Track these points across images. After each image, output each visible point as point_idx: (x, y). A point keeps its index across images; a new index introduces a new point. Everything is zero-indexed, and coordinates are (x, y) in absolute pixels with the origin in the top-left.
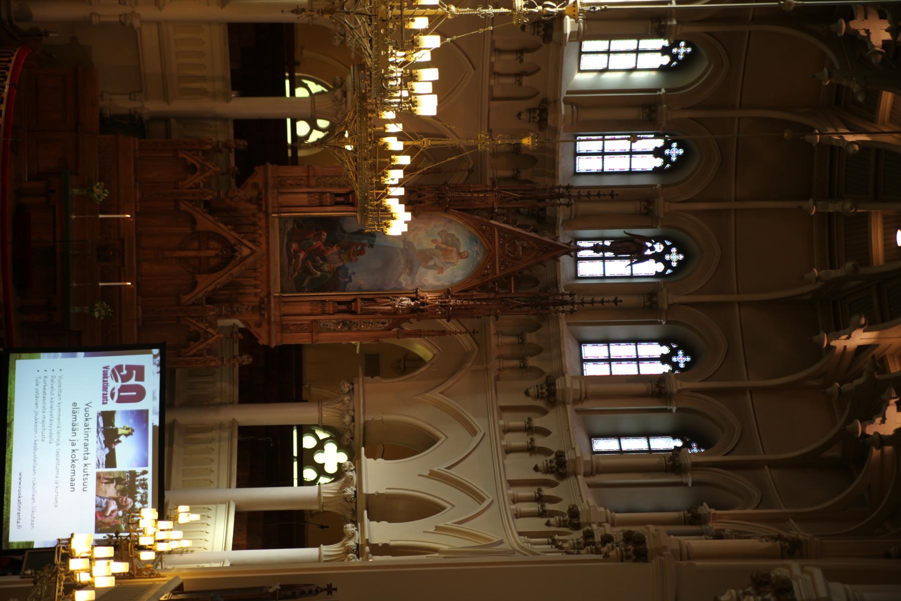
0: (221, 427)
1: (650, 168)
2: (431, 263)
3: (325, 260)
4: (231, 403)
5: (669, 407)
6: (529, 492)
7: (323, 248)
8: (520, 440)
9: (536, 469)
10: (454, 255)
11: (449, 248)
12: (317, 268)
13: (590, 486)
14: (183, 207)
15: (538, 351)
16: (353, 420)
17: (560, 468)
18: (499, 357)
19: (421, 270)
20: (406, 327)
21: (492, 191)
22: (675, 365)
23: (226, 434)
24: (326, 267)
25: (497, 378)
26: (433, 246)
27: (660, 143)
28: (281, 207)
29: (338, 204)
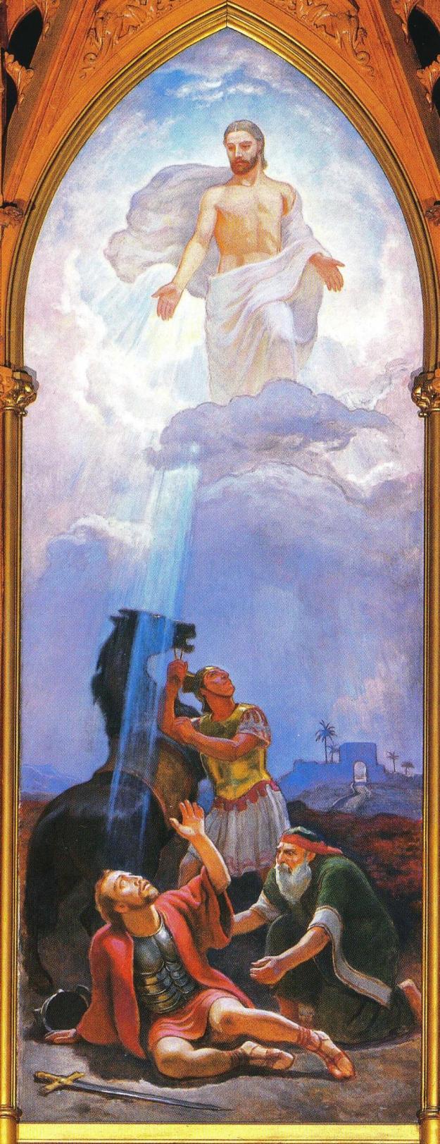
2: (282, 322)
3: (247, 886)
7: (186, 891)
10: (240, 197)
12: (291, 923)
24: (291, 877)
26: (190, 308)
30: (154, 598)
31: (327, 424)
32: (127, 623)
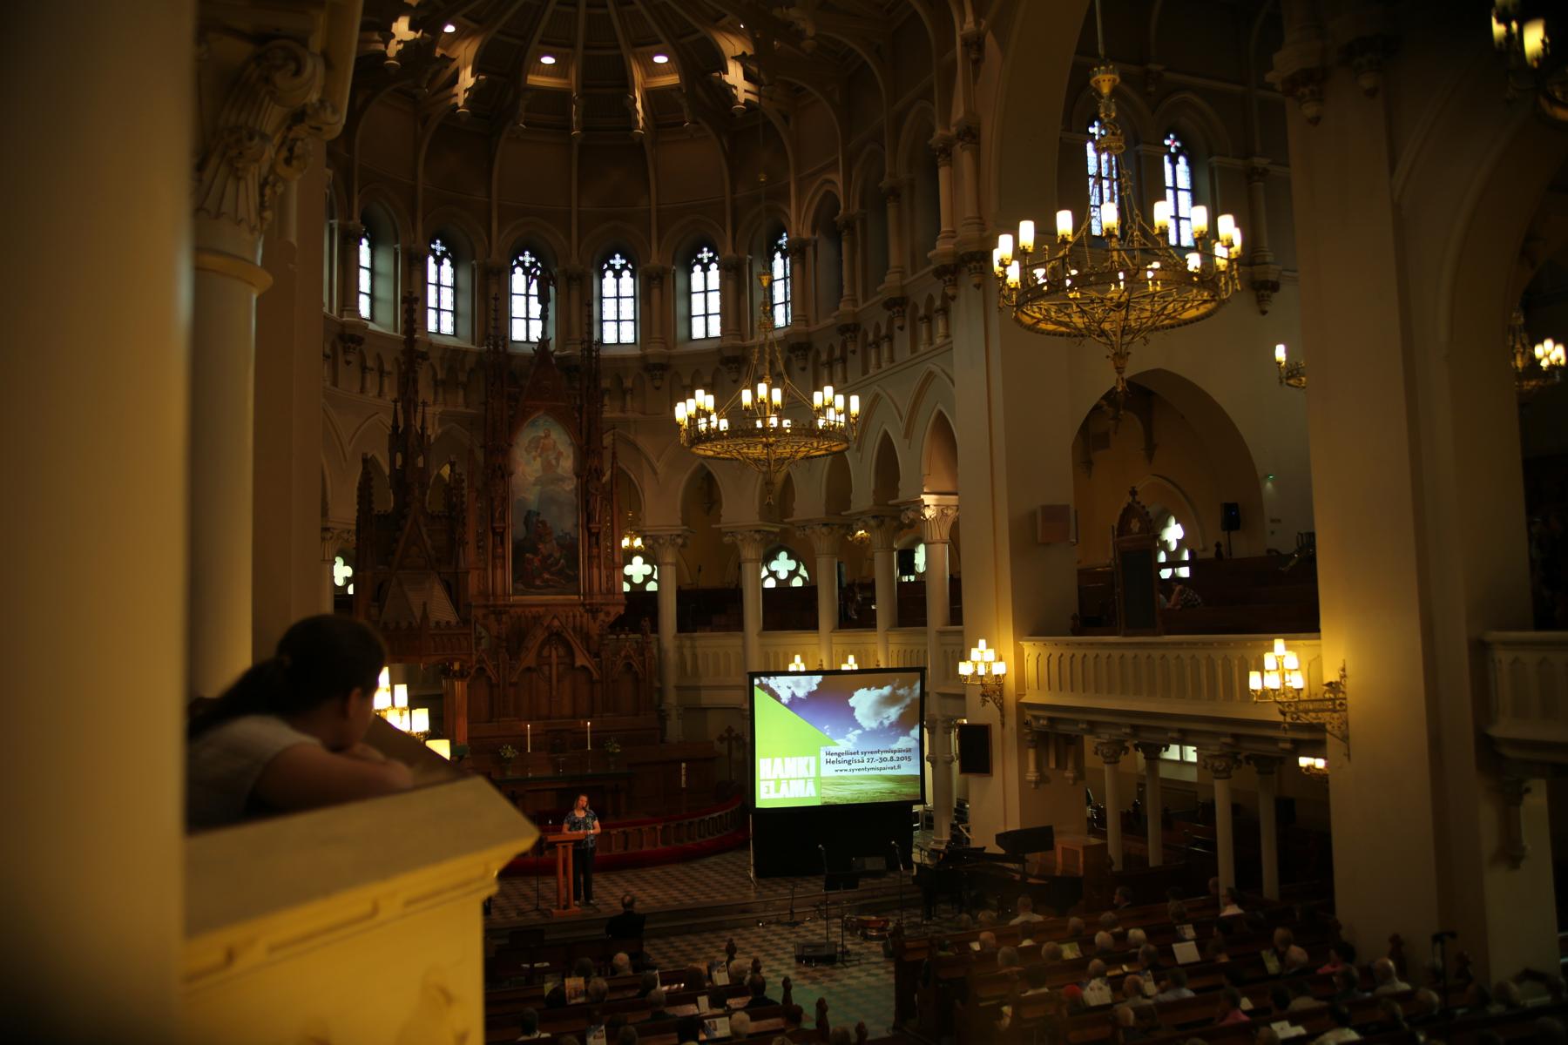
0: (680, 648)
3: (551, 555)
14: (515, 679)
19: (560, 471)
23: (688, 643)
24: (557, 555)
28: (505, 594)
29: (502, 543)
30: (534, 508)
31: (562, 479)
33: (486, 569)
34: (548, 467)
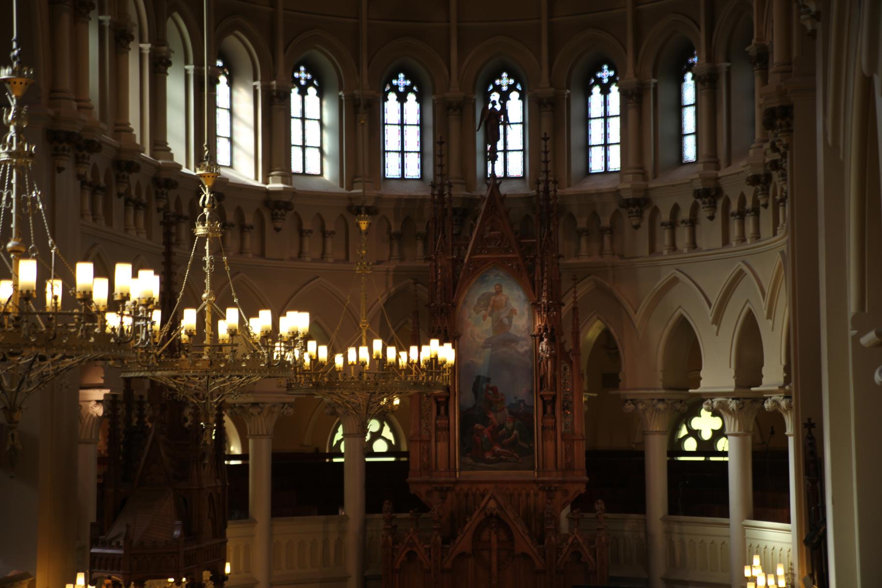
0: (668, 533)
1: (417, 106)
2: (506, 321)
3: (502, 426)
4: (645, 521)
5: (652, 86)
6: (735, 225)
8: (683, 235)
9: (711, 218)
10: (498, 298)
11: (492, 303)
13: (729, 164)
15: (595, 216)
16: (662, 400)
17: (710, 194)
18: (601, 254)
19: (512, 331)
20: (569, 346)
21: (435, 261)
22: (612, 80)
23: (676, 528)
24: (509, 425)
25: (622, 256)
26: (489, 319)
27: (392, 96)
30: (483, 373)
31: (514, 340)
32: (478, 377)
33: (430, 441)
34: (500, 326)
